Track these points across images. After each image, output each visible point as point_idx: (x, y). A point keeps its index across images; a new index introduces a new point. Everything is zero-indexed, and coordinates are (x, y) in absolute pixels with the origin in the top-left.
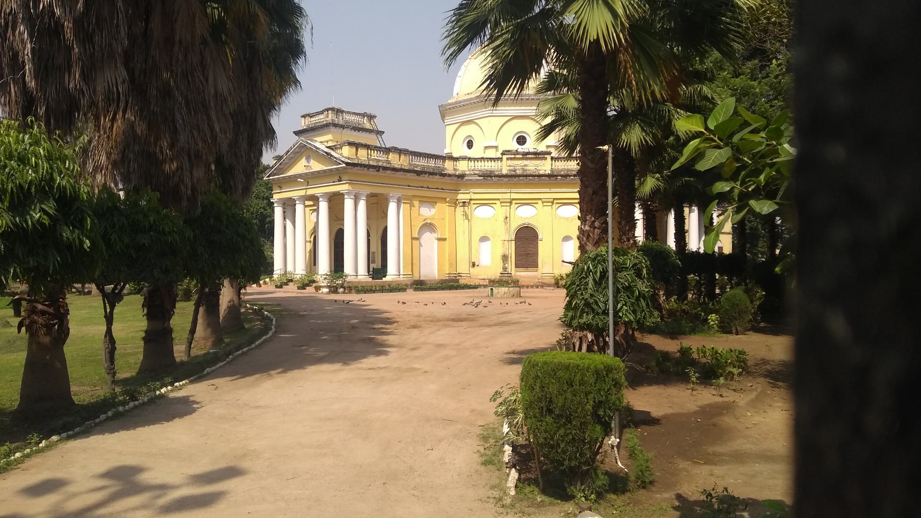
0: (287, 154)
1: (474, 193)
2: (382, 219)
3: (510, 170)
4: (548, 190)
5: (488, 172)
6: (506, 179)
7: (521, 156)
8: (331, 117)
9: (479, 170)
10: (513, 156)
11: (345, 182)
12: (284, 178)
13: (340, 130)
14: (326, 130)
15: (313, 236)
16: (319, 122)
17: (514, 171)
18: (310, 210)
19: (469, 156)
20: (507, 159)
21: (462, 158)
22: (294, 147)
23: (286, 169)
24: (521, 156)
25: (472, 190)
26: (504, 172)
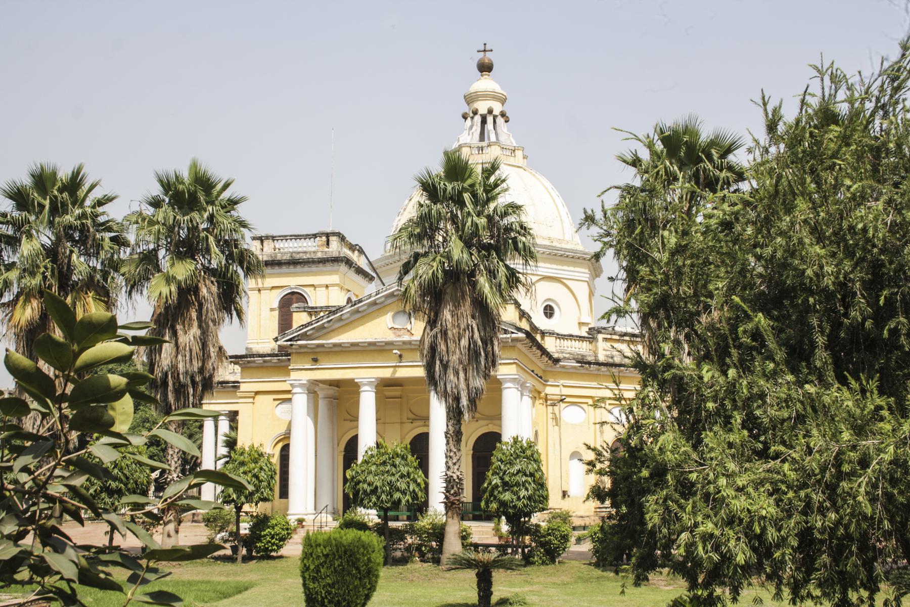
0: (355, 305)
1: (564, 386)
2: (477, 421)
3: (607, 356)
4: (594, 384)
5: (580, 357)
6: (603, 369)
7: (617, 337)
8: (335, 248)
9: (570, 353)
10: (609, 336)
11: (512, 361)
12: (322, 346)
13: (351, 274)
14: (329, 267)
15: (280, 445)
16: (305, 252)
17: (612, 358)
18: (274, 400)
19: (557, 331)
20: (605, 339)
21: (550, 333)
22: (376, 295)
23: (333, 331)
24: (617, 337)
25: (562, 382)
26: (602, 358)
